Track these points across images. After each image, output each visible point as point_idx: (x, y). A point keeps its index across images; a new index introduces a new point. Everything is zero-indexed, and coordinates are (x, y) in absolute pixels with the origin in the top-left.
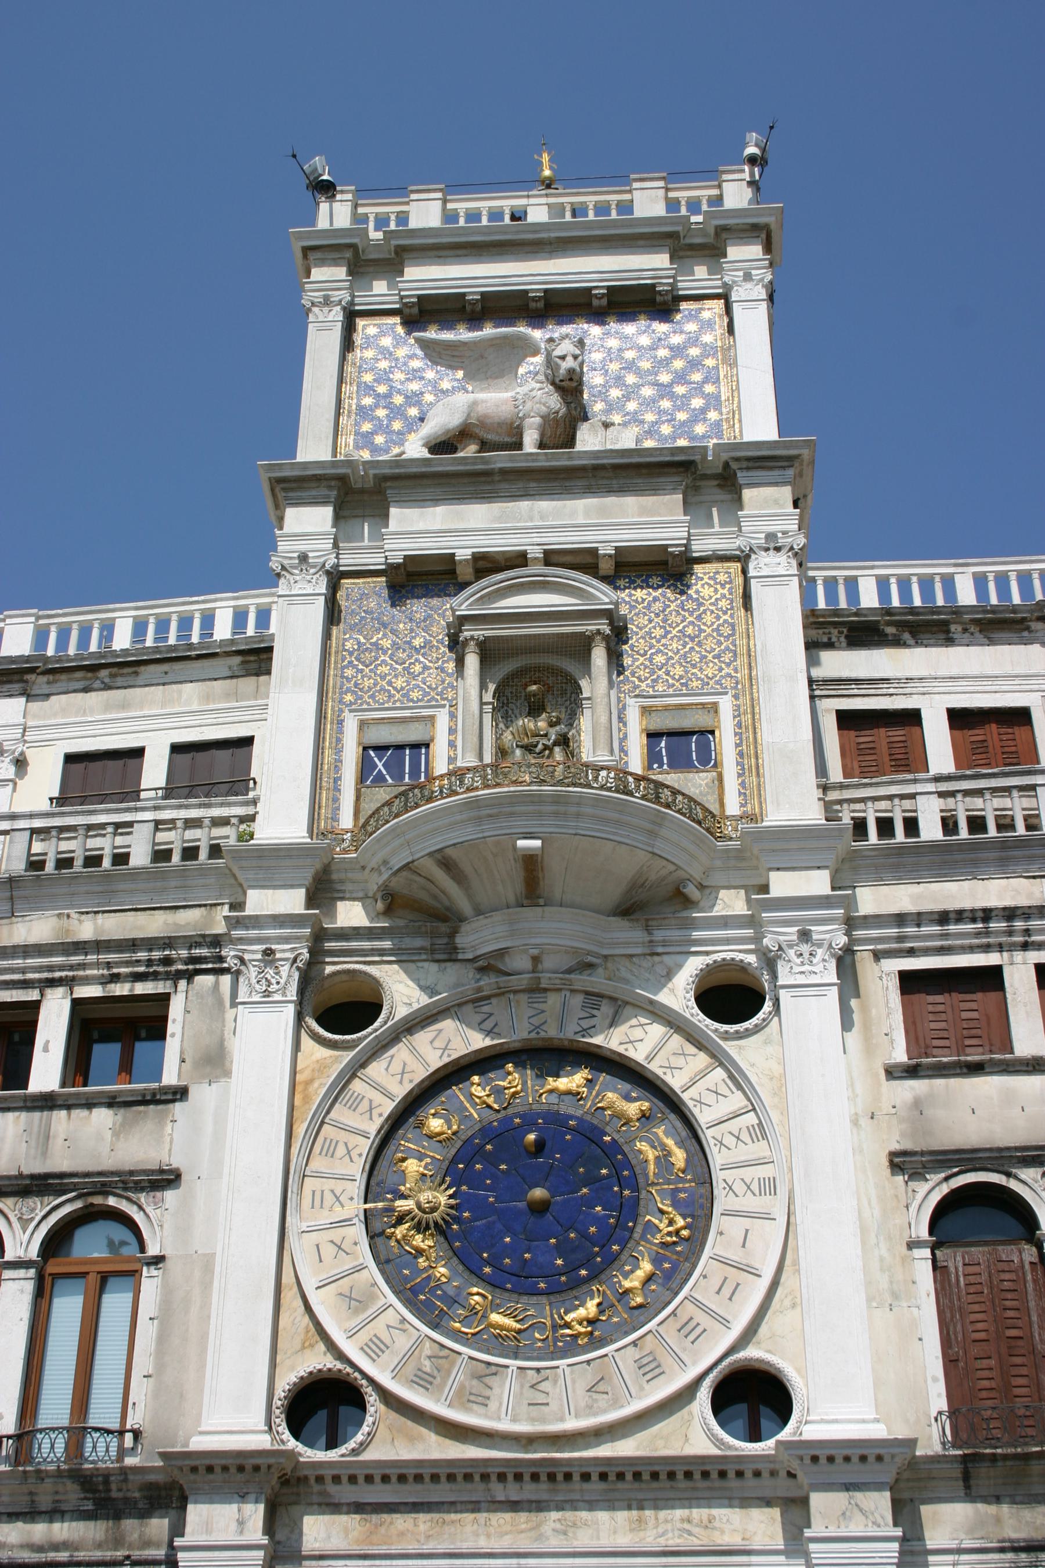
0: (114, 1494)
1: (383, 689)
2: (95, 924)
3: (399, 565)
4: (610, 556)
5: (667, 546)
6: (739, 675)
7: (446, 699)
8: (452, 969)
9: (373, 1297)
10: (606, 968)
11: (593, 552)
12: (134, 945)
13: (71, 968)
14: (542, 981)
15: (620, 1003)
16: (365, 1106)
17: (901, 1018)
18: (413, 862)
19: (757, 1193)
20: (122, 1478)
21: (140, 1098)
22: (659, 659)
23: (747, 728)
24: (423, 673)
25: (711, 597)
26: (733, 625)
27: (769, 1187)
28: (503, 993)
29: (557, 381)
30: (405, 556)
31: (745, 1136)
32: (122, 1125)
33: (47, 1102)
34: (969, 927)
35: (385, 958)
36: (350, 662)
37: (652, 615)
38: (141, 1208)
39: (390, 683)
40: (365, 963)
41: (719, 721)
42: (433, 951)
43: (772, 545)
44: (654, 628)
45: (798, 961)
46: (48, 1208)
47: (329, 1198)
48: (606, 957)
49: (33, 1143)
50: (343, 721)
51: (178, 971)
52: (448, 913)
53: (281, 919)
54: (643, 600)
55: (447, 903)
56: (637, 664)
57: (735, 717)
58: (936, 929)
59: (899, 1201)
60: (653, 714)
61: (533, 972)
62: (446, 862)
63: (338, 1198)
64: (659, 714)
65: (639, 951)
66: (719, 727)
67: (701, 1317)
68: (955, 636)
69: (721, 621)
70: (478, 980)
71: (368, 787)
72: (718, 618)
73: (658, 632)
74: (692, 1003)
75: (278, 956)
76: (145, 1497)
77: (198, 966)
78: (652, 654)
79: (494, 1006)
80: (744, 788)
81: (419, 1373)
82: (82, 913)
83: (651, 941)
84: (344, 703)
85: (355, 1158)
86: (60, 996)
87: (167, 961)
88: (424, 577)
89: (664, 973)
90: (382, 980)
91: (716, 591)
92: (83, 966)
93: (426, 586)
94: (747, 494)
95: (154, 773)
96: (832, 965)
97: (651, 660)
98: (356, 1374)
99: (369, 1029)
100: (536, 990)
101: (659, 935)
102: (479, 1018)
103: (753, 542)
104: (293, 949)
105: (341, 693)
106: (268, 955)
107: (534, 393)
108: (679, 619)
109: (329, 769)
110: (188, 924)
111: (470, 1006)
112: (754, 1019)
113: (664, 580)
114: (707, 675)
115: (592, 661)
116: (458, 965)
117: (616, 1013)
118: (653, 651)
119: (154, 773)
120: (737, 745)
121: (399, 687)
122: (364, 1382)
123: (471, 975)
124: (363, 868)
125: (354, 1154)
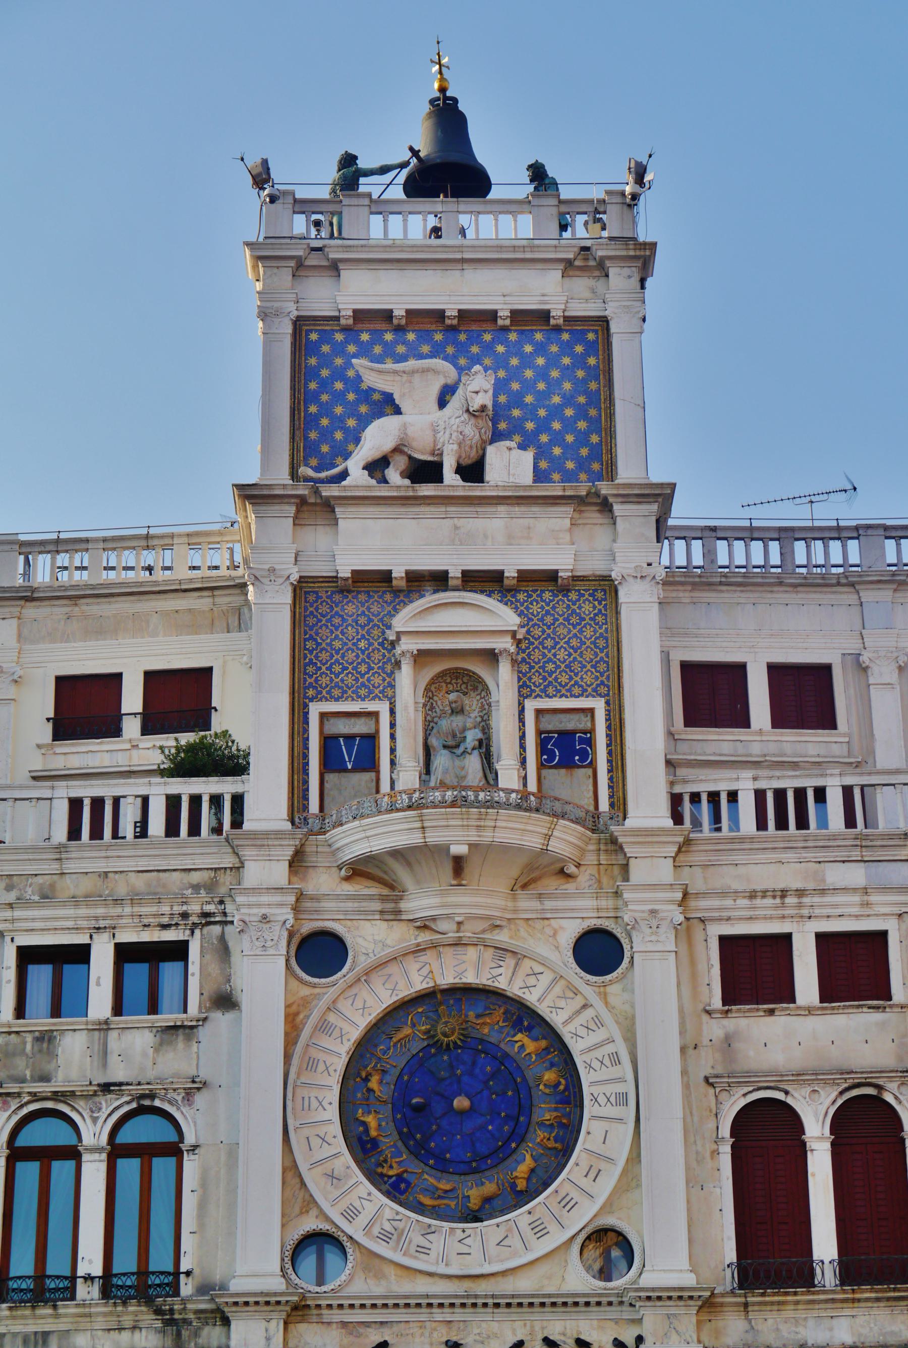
0: (176, 1316)
1: (337, 685)
3: (346, 579)
4: (514, 578)
6: (610, 684)
7: (387, 696)
9: (348, 1177)
11: (501, 573)
15: (519, 956)
16: (336, 1033)
17: (719, 972)
19: (614, 1104)
20: (182, 1306)
21: (172, 1024)
22: (550, 667)
23: (615, 730)
24: (367, 673)
27: (622, 1100)
29: (471, 409)
30: (353, 571)
31: (607, 1061)
32: (161, 1044)
33: (104, 1027)
36: (311, 660)
38: (178, 1109)
39: (342, 681)
42: (382, 912)
43: (639, 576)
45: (650, 930)
46: (111, 1108)
47: (314, 1104)
48: (509, 919)
49: (95, 1058)
50: (308, 713)
51: (193, 923)
54: (538, 613)
55: (395, 878)
57: (607, 720)
59: (711, 1111)
62: (396, 854)
63: (320, 1103)
67: (575, 1194)
69: (598, 635)
70: (416, 937)
73: (549, 643)
74: (571, 960)
76: (199, 1318)
77: (208, 919)
78: (545, 662)
79: (429, 956)
80: (612, 782)
81: (382, 1232)
84: (308, 698)
85: (332, 1073)
87: (185, 915)
88: (366, 584)
89: (551, 934)
91: (594, 607)
92: (120, 917)
93: (368, 592)
95: (132, 699)
97: (543, 667)
98: (339, 1233)
99: (339, 974)
100: (458, 944)
101: (549, 904)
102: (418, 966)
106: (265, 918)
107: (452, 421)
108: (565, 632)
109: (299, 753)
111: (411, 957)
112: (615, 973)
113: (555, 596)
114: (586, 683)
117: (517, 964)
119: (132, 699)
120: (608, 745)
122: (345, 1238)
123: (411, 932)
125: (331, 1069)
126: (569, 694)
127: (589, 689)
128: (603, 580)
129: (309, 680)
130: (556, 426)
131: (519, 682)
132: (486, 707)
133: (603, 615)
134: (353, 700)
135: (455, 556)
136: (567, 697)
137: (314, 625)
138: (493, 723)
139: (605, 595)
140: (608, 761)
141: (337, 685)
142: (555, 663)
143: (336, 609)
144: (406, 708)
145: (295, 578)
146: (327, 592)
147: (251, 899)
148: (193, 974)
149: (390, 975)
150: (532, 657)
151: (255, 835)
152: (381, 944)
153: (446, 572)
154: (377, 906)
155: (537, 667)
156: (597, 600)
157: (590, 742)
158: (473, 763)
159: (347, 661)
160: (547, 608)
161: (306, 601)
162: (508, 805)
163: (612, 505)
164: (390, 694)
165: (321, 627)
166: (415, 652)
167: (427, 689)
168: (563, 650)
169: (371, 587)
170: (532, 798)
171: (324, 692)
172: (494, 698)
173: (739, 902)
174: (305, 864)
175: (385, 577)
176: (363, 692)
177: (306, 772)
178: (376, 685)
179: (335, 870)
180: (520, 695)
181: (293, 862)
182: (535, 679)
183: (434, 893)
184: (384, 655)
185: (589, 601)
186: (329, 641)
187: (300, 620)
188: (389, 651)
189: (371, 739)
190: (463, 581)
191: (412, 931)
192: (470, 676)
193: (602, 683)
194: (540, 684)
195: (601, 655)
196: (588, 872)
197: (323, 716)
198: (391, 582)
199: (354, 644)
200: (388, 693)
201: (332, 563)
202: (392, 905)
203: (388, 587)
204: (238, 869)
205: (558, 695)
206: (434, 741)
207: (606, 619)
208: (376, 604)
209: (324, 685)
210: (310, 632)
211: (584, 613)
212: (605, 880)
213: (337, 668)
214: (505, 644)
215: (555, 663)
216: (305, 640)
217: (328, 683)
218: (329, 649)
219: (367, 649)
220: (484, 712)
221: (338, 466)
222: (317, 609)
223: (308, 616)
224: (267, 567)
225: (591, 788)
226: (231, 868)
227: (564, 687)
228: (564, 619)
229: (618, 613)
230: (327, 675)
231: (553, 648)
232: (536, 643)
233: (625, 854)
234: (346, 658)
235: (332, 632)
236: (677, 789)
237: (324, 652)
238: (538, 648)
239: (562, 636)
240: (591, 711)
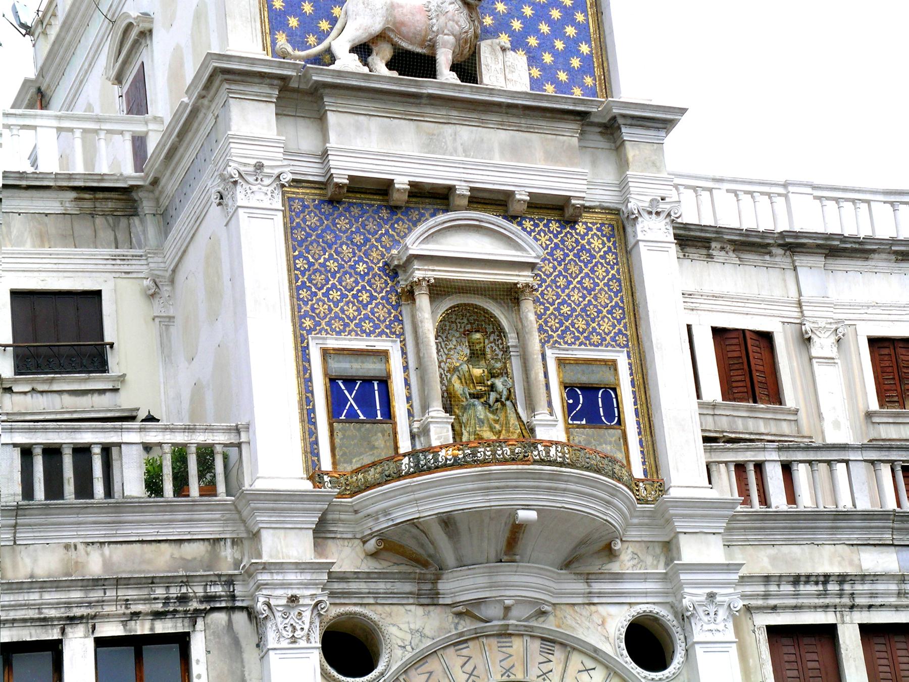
1: (337, 316)
2: (103, 555)
4: (524, 201)
5: (569, 198)
6: (628, 333)
7: (394, 333)
8: (435, 612)
10: (555, 616)
11: (510, 194)
12: (153, 583)
13: (90, 604)
14: (510, 627)
22: (565, 309)
24: (369, 303)
25: (600, 250)
26: (619, 281)
28: (478, 637)
34: (811, 588)
35: (379, 601)
36: (303, 283)
37: (556, 263)
40: (361, 604)
41: (618, 379)
42: (419, 595)
48: (554, 604)
50: (307, 347)
53: (303, 566)
56: (548, 312)
58: (787, 588)
60: (568, 367)
61: (503, 619)
64: (572, 367)
65: (580, 601)
66: (619, 385)
68: (714, 253)
71: (342, 421)
72: (607, 272)
73: (562, 282)
75: (301, 601)
82: (88, 544)
83: (590, 593)
84: (304, 329)
86: (82, 634)
88: (358, 195)
90: (380, 624)
91: (604, 244)
93: (361, 205)
94: (631, 152)
96: (730, 625)
97: (558, 309)
101: (597, 587)
103: (640, 204)
104: (312, 596)
106: (293, 601)
110: (195, 559)
111: (451, 650)
114: (604, 330)
116: (439, 608)
121: (351, 316)
123: (450, 618)
124: (356, 512)
128: (609, 213)
130: (544, 28)
134: (357, 334)
136: (585, 345)
137: (303, 240)
142: (569, 305)
146: (314, 200)
147: (275, 577)
148: (199, 676)
149: (431, 673)
152: (418, 635)
153: (451, 189)
154: (408, 587)
155: (551, 308)
159: (345, 287)
160: (555, 241)
163: (619, 128)
165: (311, 243)
166: (433, 281)
171: (323, 323)
173: (782, 588)
175: (383, 188)
176: (367, 326)
179: (357, 542)
182: (552, 322)
183: (481, 571)
185: (597, 236)
186: (322, 261)
191: (451, 618)
199: (351, 267)
202: (429, 586)
205: (577, 343)
208: (371, 220)
209: (322, 315)
215: (569, 305)
216: (295, 258)
219: (367, 274)
221: (310, 47)
224: (253, 162)
227: (582, 334)
228: (574, 255)
232: (548, 280)
237: (318, 274)
238: (551, 287)
239: (574, 275)
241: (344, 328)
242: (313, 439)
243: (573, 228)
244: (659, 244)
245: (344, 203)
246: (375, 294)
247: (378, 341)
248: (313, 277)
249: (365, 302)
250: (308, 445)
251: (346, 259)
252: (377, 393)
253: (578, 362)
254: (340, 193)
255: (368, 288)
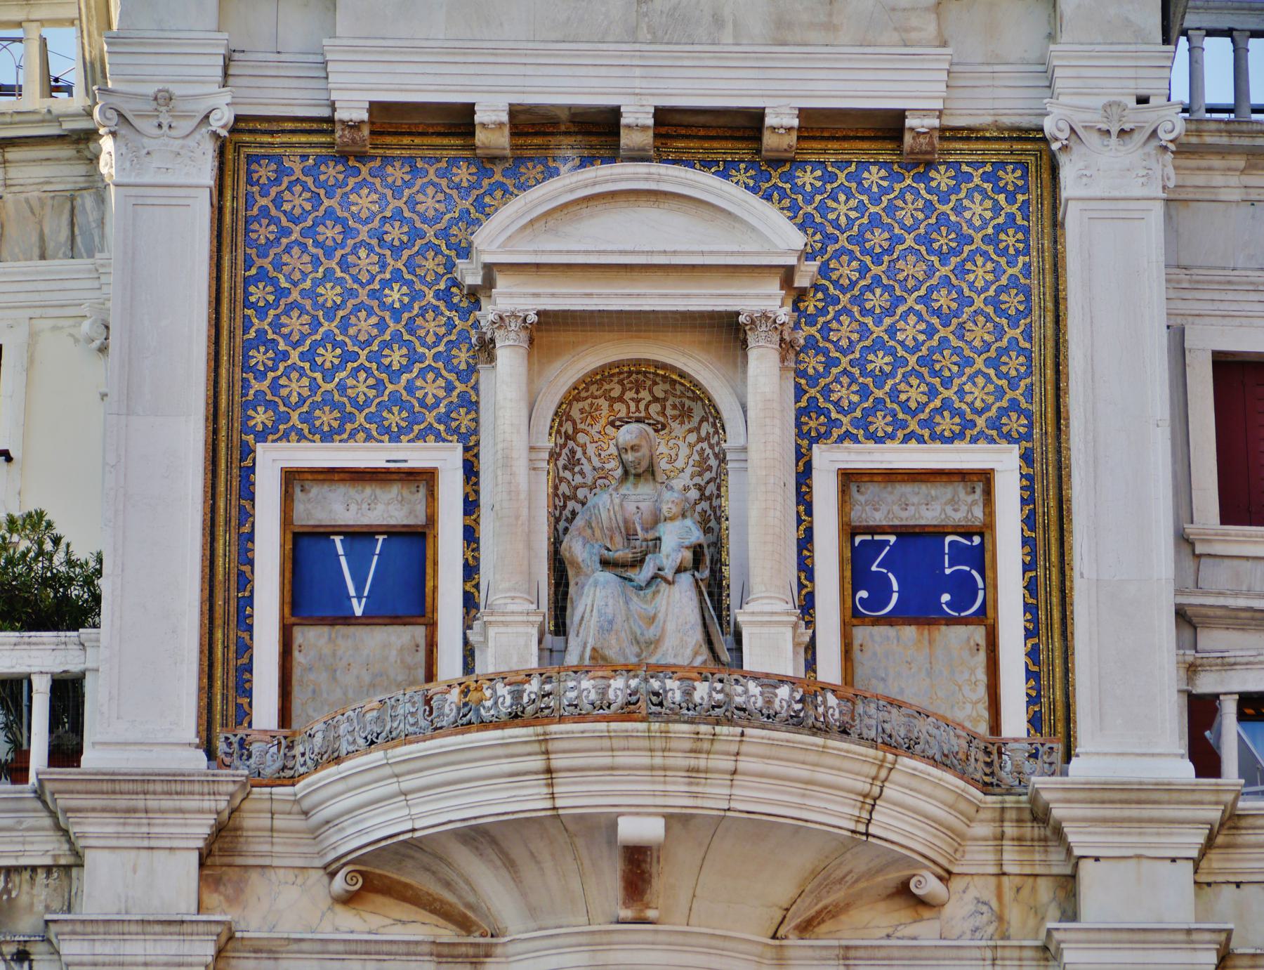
1: (328, 401)
3: (356, 126)
4: (790, 129)
5: (901, 115)
6: (1035, 408)
7: (456, 431)
11: (757, 116)
18: (414, 830)
22: (880, 361)
23: (1046, 529)
24: (406, 369)
30: (373, 105)
39: (342, 388)
43: (1115, 130)
44: (869, 288)
50: (252, 469)
52: (469, 913)
55: (471, 899)
56: (834, 371)
62: (478, 836)
73: (877, 300)
80: (1036, 662)
84: (252, 430)
88: (406, 140)
91: (997, 209)
93: (411, 160)
97: (861, 363)
105: (245, 406)
113: (894, 177)
115: (750, 380)
118: (868, 343)
120: (1027, 567)
126: (926, 433)
127: (981, 422)
128: (1019, 139)
129: (256, 386)
131: (798, 400)
132: (713, 462)
133: (1020, 229)
134: (370, 437)
135: (638, 72)
136: (921, 440)
138: (730, 505)
139: (1024, 176)
140: (1027, 608)
141: (328, 401)
142: (892, 352)
143: (327, 203)
144: (507, 463)
145: (222, 119)
146: (304, 157)
147: (99, 948)
150: (833, 336)
151: (112, 782)
155: (845, 361)
156: (1003, 190)
157: (979, 557)
158: (679, 606)
159: (354, 339)
161: (250, 182)
162: (769, 718)
164: (465, 422)
166: (533, 318)
167: (561, 415)
168: (912, 319)
169: (418, 147)
170: (832, 700)
171: (295, 416)
172: (734, 437)
174: (239, 861)
176: (394, 418)
177: (245, 623)
178: (430, 400)
180: (800, 434)
181: (210, 853)
182: (840, 392)
184: (450, 325)
187: (234, 230)
188: (465, 314)
189: (415, 540)
190: (656, 136)
192: (674, 382)
193: (1014, 404)
194: (853, 407)
195: (1011, 333)
196: (973, 893)
197: (292, 479)
198: (472, 134)
199: (373, 294)
200: (462, 423)
201: (321, 84)
203: (464, 147)
204: (67, 869)
206: (577, 549)
207: (1026, 241)
210: (259, 262)
211: (969, 222)
212: (1014, 915)
213: (329, 356)
214: (767, 299)
215: (892, 352)
217: (306, 392)
218: (308, 304)
219: (407, 307)
220: (707, 476)
222: (278, 201)
223: (256, 219)
225: (981, 676)
226: (49, 869)
227: (914, 414)
229: (1057, 224)
230: (302, 373)
231: (890, 312)
233: (1069, 850)
234: (352, 331)
235: (316, 262)
236: (1206, 684)
237: (295, 313)
238: (849, 313)
240: (985, 478)
241: (342, 426)
242: (245, 660)
243: (922, 177)
244: (1122, 205)
245: (374, 158)
246: (421, 350)
247: (412, 449)
248: (284, 319)
249: (396, 367)
250: (232, 672)
251: (364, 277)
252: (343, 560)
253: (891, 476)
254: (353, 140)
255: (406, 337)
